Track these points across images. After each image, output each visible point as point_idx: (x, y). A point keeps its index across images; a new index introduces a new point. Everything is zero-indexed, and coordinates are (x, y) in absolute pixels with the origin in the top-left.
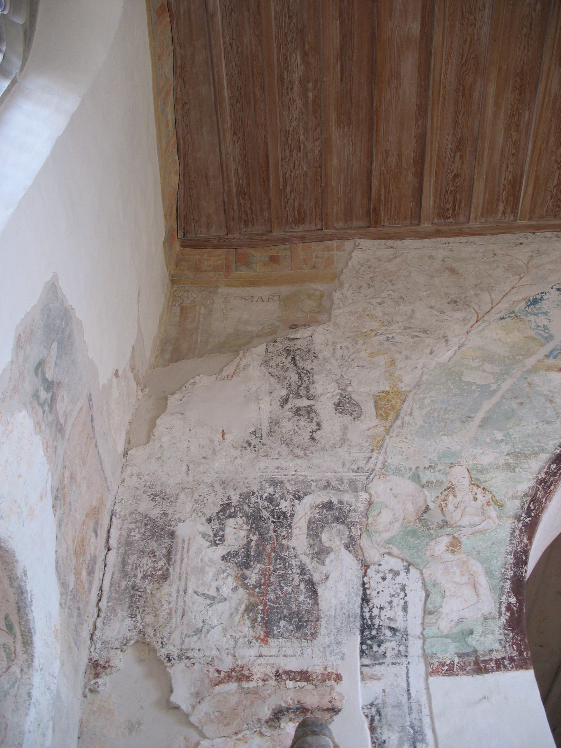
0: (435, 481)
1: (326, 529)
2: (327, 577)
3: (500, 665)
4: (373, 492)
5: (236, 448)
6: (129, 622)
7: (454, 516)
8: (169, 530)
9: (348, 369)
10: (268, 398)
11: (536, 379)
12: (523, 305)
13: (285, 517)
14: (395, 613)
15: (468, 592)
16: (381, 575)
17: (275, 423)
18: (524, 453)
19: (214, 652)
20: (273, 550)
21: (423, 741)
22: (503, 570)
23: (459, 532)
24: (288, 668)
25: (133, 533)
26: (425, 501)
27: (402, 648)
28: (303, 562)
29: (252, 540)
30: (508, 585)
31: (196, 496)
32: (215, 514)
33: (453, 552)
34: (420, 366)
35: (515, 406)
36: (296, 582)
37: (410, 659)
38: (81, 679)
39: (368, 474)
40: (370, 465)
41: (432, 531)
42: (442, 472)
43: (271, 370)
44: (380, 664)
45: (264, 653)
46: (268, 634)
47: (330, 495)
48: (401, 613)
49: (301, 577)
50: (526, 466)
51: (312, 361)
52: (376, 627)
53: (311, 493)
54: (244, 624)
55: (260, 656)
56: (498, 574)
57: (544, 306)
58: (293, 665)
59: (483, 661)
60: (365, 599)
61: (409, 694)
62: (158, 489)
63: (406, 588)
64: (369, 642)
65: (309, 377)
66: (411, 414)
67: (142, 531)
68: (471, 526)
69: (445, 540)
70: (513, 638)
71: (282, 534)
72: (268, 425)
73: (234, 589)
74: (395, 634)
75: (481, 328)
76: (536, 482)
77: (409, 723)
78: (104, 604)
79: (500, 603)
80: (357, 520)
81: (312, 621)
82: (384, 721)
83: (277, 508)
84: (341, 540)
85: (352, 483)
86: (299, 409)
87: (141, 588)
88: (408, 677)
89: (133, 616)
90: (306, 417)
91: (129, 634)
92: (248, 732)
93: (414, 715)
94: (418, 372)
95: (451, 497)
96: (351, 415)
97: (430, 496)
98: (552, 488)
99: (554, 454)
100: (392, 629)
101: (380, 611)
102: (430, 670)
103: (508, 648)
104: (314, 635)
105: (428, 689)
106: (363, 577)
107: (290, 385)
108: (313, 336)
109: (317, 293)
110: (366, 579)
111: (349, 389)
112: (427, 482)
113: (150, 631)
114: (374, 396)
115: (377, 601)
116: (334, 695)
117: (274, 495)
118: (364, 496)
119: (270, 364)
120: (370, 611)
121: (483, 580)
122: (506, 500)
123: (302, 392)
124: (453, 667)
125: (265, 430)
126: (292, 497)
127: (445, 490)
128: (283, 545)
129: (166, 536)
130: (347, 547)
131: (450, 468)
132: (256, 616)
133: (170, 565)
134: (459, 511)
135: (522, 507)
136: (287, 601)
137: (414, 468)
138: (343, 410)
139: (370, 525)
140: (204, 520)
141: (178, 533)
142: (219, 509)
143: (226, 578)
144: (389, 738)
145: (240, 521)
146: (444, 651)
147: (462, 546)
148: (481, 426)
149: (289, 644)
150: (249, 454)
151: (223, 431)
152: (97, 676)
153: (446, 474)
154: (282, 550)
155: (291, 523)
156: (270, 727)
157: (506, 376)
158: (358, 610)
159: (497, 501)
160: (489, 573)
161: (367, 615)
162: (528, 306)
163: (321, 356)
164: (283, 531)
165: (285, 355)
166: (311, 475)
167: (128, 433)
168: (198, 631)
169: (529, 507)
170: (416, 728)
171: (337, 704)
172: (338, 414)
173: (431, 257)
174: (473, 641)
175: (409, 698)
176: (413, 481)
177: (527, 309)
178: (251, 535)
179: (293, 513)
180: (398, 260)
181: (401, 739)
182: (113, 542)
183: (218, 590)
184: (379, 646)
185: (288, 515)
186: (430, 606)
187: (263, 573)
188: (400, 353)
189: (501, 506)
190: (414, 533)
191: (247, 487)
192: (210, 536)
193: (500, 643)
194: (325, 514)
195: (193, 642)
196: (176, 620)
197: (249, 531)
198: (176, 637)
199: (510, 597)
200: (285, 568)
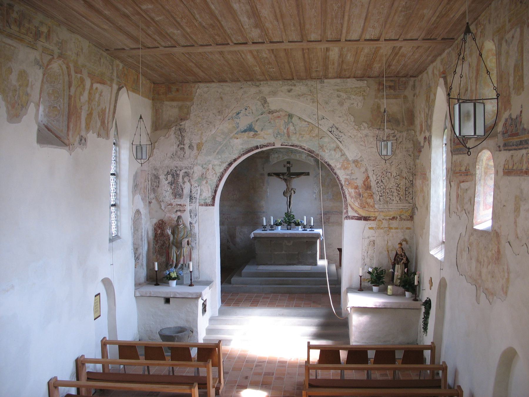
3: (210, 205)
7: (208, 177)
12: (235, 114)
15: (207, 192)
17: (177, 152)
34: (207, 135)
35: (225, 149)
57: (240, 115)
58: (179, 203)
60: (191, 192)
62: (156, 168)
68: (210, 178)
69: (205, 181)
85: (190, 167)
86: (181, 148)
89: (154, 194)
94: (207, 137)
100: (195, 197)
109: (188, 106)
111: (192, 142)
113: (157, 196)
115: (193, 192)
118: (192, 170)
121: (210, 190)
123: (182, 143)
125: (175, 154)
136: (178, 192)
145: (171, 175)
150: (172, 160)
160: (211, 188)
166: (183, 165)
168: (165, 197)
173: (217, 92)
174: (206, 200)
187: (174, 187)
189: (216, 174)
190: (200, 179)
195: (164, 199)
196: (161, 195)
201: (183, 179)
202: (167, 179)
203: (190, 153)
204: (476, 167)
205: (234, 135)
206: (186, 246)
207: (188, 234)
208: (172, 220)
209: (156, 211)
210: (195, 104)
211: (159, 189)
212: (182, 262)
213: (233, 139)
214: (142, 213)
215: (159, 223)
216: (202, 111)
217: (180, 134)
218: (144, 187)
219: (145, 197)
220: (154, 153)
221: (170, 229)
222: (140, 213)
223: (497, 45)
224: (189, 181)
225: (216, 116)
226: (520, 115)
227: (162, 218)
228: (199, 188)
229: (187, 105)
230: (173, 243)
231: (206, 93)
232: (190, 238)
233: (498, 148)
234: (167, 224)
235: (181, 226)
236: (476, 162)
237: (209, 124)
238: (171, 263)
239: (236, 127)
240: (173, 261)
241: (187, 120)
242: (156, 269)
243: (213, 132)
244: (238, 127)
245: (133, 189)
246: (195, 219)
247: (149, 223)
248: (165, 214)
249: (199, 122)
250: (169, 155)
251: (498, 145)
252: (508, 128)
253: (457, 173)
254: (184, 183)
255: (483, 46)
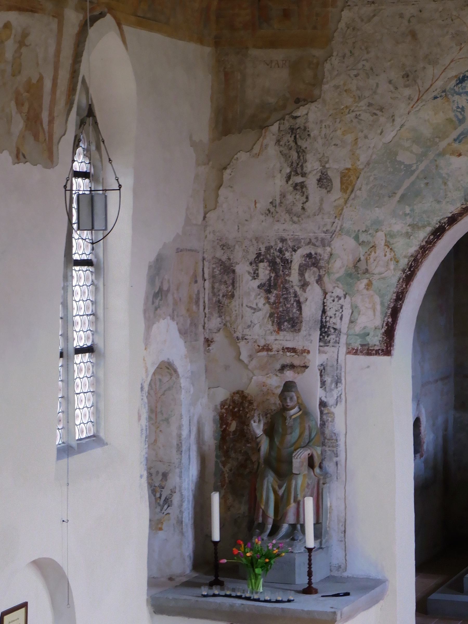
0: (366, 241)
1: (308, 271)
2: (307, 300)
3: (377, 353)
4: (333, 247)
5: (262, 214)
6: (219, 319)
7: (373, 267)
8: (232, 269)
9: (327, 148)
10: (279, 175)
11: (442, 162)
12: (454, 82)
13: (288, 263)
14: (337, 321)
15: (370, 313)
16: (332, 299)
17: (283, 196)
18: (418, 225)
19: (256, 337)
20: (282, 283)
21: (340, 382)
22: (389, 303)
23: (372, 278)
24: (288, 346)
25: (215, 271)
26: (360, 254)
27: (337, 339)
28: (296, 290)
29: (271, 277)
30: (390, 311)
31: (244, 247)
32: (253, 260)
33: (367, 289)
34: (372, 146)
35: (422, 186)
36: (292, 302)
37: (340, 345)
38: (202, 349)
39: (332, 234)
40: (333, 228)
41: (359, 275)
42: (371, 235)
43: (282, 149)
44: (327, 346)
45: (277, 338)
46: (280, 329)
47: (311, 248)
48: (339, 321)
49: (295, 299)
50: (417, 235)
51: (306, 140)
52: (327, 327)
53: (301, 248)
54: (269, 323)
55: (276, 340)
56: (386, 305)
58: (290, 345)
59: (371, 350)
60: (324, 312)
61: (338, 362)
63: (343, 307)
64: (323, 334)
65: (303, 156)
66: (360, 189)
67: (219, 269)
68: (380, 274)
69: (365, 281)
70: (385, 340)
71: (286, 273)
72: (279, 197)
73: (264, 304)
74: (335, 332)
75: (419, 107)
76: (420, 247)
77: (335, 374)
78: (207, 310)
79: (384, 321)
80: (324, 265)
81: (299, 323)
82: (326, 373)
83: (284, 256)
84: (315, 277)
85: (323, 240)
86: (296, 185)
87: (222, 302)
88: (338, 354)
89: (220, 316)
90: (300, 191)
91: (220, 326)
92: (271, 374)
93: (338, 371)
95: (373, 253)
96: (326, 189)
97: (362, 251)
98: (427, 252)
99: (435, 228)
100: (335, 329)
101: (330, 319)
102: (348, 351)
103: (382, 345)
104: (299, 330)
105: (345, 359)
106: (324, 299)
107: (292, 163)
108: (309, 114)
109: (315, 61)
110: (325, 300)
111: (327, 166)
112: (363, 242)
113: (228, 324)
114: (342, 173)
115: (330, 313)
116: (306, 360)
117: (282, 248)
118: (328, 249)
119: (281, 143)
120: (326, 318)
121: (378, 307)
122: (401, 258)
123: (299, 170)
124: (358, 351)
125: (278, 201)
126: (291, 250)
127: (371, 248)
128: (286, 280)
129: (231, 272)
130: (317, 282)
131: (376, 232)
132: (274, 320)
133: (234, 289)
134: (375, 263)
135: (408, 264)
137: (357, 231)
138: (322, 185)
139: (330, 268)
140: (248, 263)
141: (236, 271)
142: (255, 256)
143: (260, 298)
144: (327, 380)
146: (355, 342)
147: (373, 286)
148: (399, 201)
149: (288, 334)
150: (270, 219)
151: (255, 201)
152: (209, 346)
153: (373, 236)
154: (286, 283)
155: (291, 266)
156: (280, 372)
157: (424, 158)
158: (320, 318)
159: (396, 258)
160: (382, 304)
161: (324, 320)
162: (457, 84)
163: (312, 135)
164: (286, 272)
165: (291, 133)
166: (301, 235)
167: (204, 200)
168: (249, 326)
169: (411, 264)
170: (338, 377)
171: (307, 365)
172: (319, 188)
175: (337, 363)
176: (355, 240)
177: (455, 88)
178: (271, 273)
179: (292, 260)
180: (376, 19)
181: (332, 381)
182: (206, 276)
183: (257, 305)
184: (328, 337)
185: (289, 261)
186: (352, 319)
187: (277, 296)
188: (362, 132)
190: (350, 275)
191: (269, 243)
192: (252, 273)
193: (379, 342)
194: (308, 261)
195: (247, 331)
197: (270, 270)
198: (240, 328)
199: (389, 318)
200: (287, 294)
201: (301, 273)
202: (255, 275)
203: (322, 200)
205: (449, 144)
206: (306, 472)
207: (313, 435)
208: (269, 392)
209: (227, 367)
210: (335, 54)
211: (235, 303)
212: (291, 518)
213: (448, 156)
214: (180, 370)
215: (233, 401)
216: (356, 76)
217: (293, 144)
218: (190, 298)
219: (194, 324)
220: (221, 199)
221: (259, 421)
222: (176, 371)
224: (319, 280)
225: (396, 88)
227: (240, 388)
228: (346, 303)
229: (314, 56)
230: (268, 462)
231: (369, 20)
232: (319, 450)
234: (255, 404)
235: (292, 412)
237: (375, 114)
238: (260, 520)
239: (454, 119)
240: (265, 516)
241: (312, 102)
242: (216, 536)
243: (388, 137)
244: (461, 121)
245: (145, 304)
246: (335, 393)
247: (205, 400)
248: (251, 375)
249: (347, 107)
250: (263, 204)
254: (304, 285)
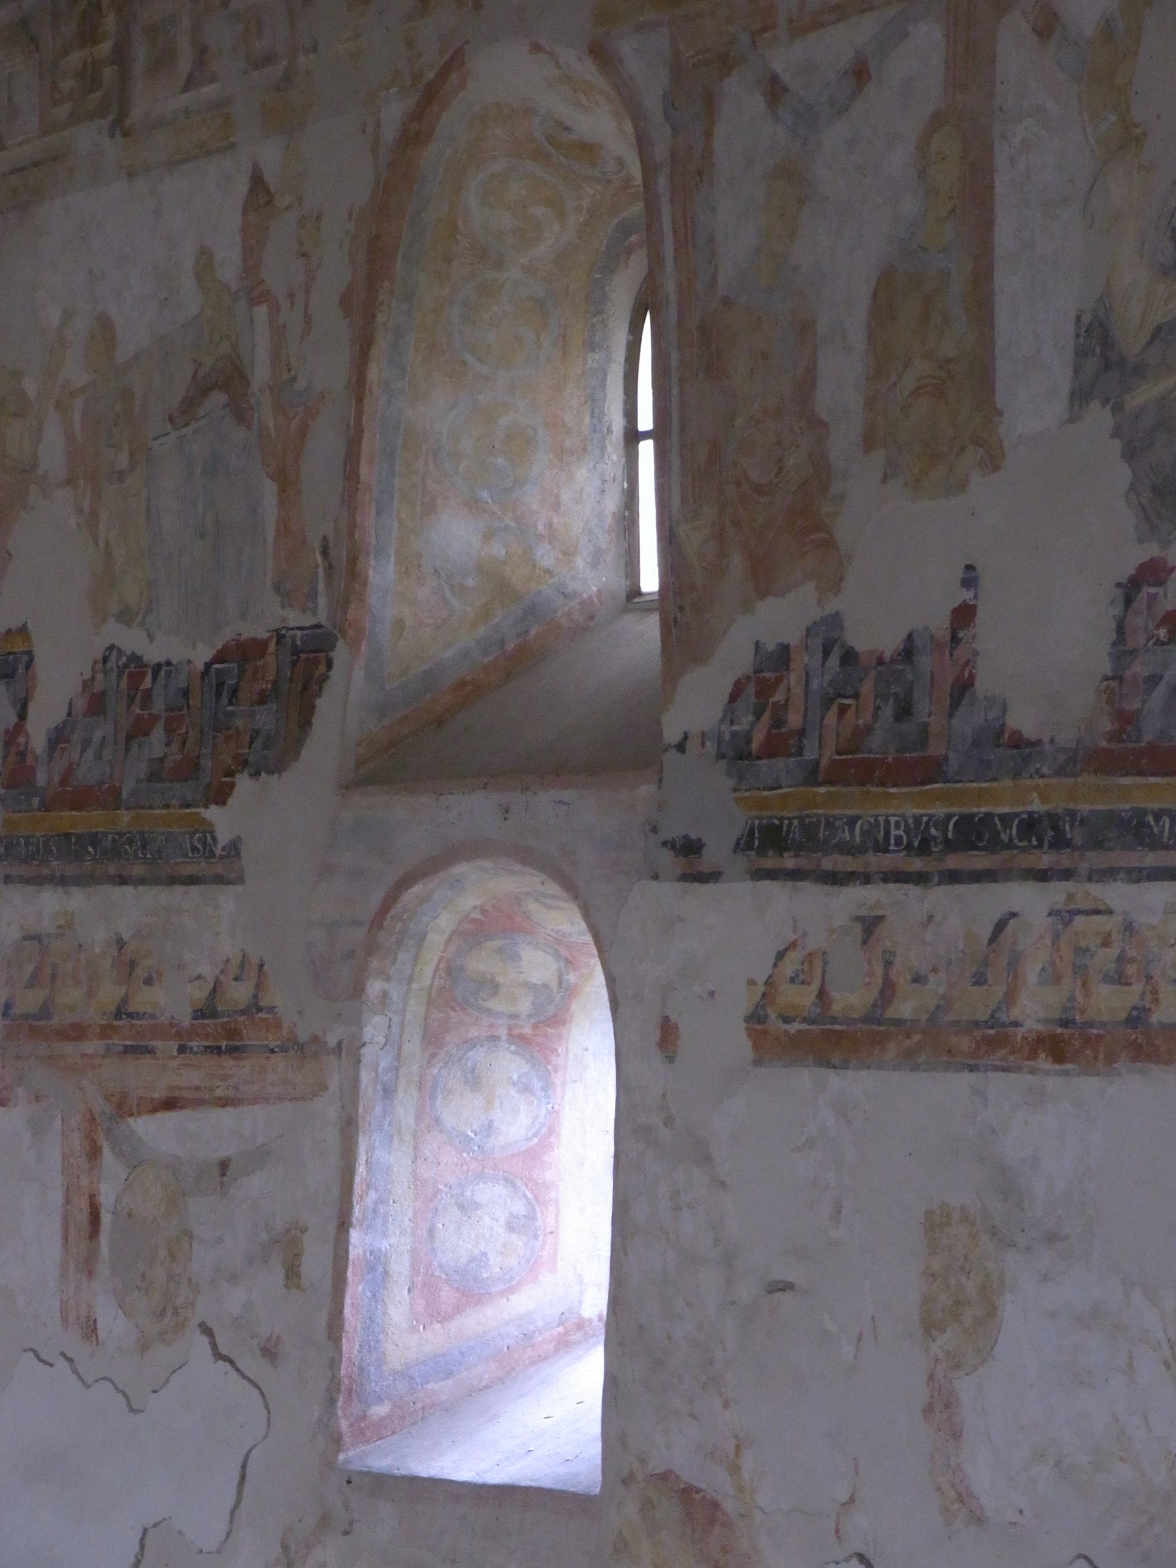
204: (358, 989)
223: (652, 100)
226: (955, 640)
233: (666, 858)
236: (371, 948)
251: (675, 829)
252: (794, 719)
253: (77, 1032)
255: (454, 77)
